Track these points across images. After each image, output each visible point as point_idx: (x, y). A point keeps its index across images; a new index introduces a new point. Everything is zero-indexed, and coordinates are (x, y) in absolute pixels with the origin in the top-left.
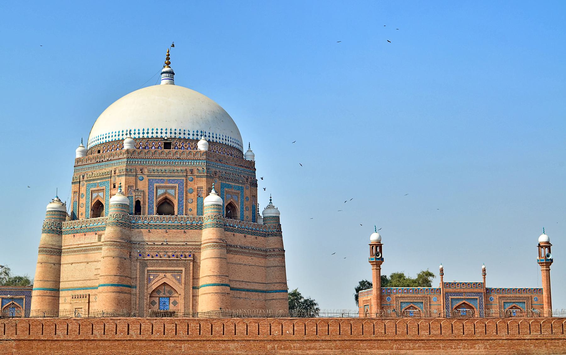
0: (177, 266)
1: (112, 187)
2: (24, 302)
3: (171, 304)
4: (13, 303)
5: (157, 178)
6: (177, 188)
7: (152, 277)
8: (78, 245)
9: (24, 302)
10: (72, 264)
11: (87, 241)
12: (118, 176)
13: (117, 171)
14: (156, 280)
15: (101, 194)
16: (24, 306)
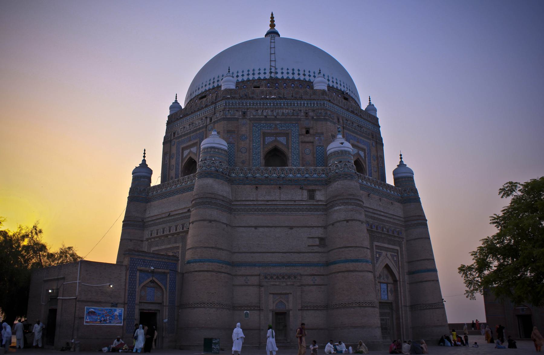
0: (394, 245)
1: (304, 131)
2: (168, 279)
3: (389, 293)
4: (152, 282)
5: (352, 134)
6: (366, 151)
7: (378, 256)
8: (268, 201)
9: (168, 279)
10: (256, 227)
11: (283, 197)
12: (317, 120)
13: (311, 114)
14: (380, 259)
15: (282, 140)
16: (168, 286)
